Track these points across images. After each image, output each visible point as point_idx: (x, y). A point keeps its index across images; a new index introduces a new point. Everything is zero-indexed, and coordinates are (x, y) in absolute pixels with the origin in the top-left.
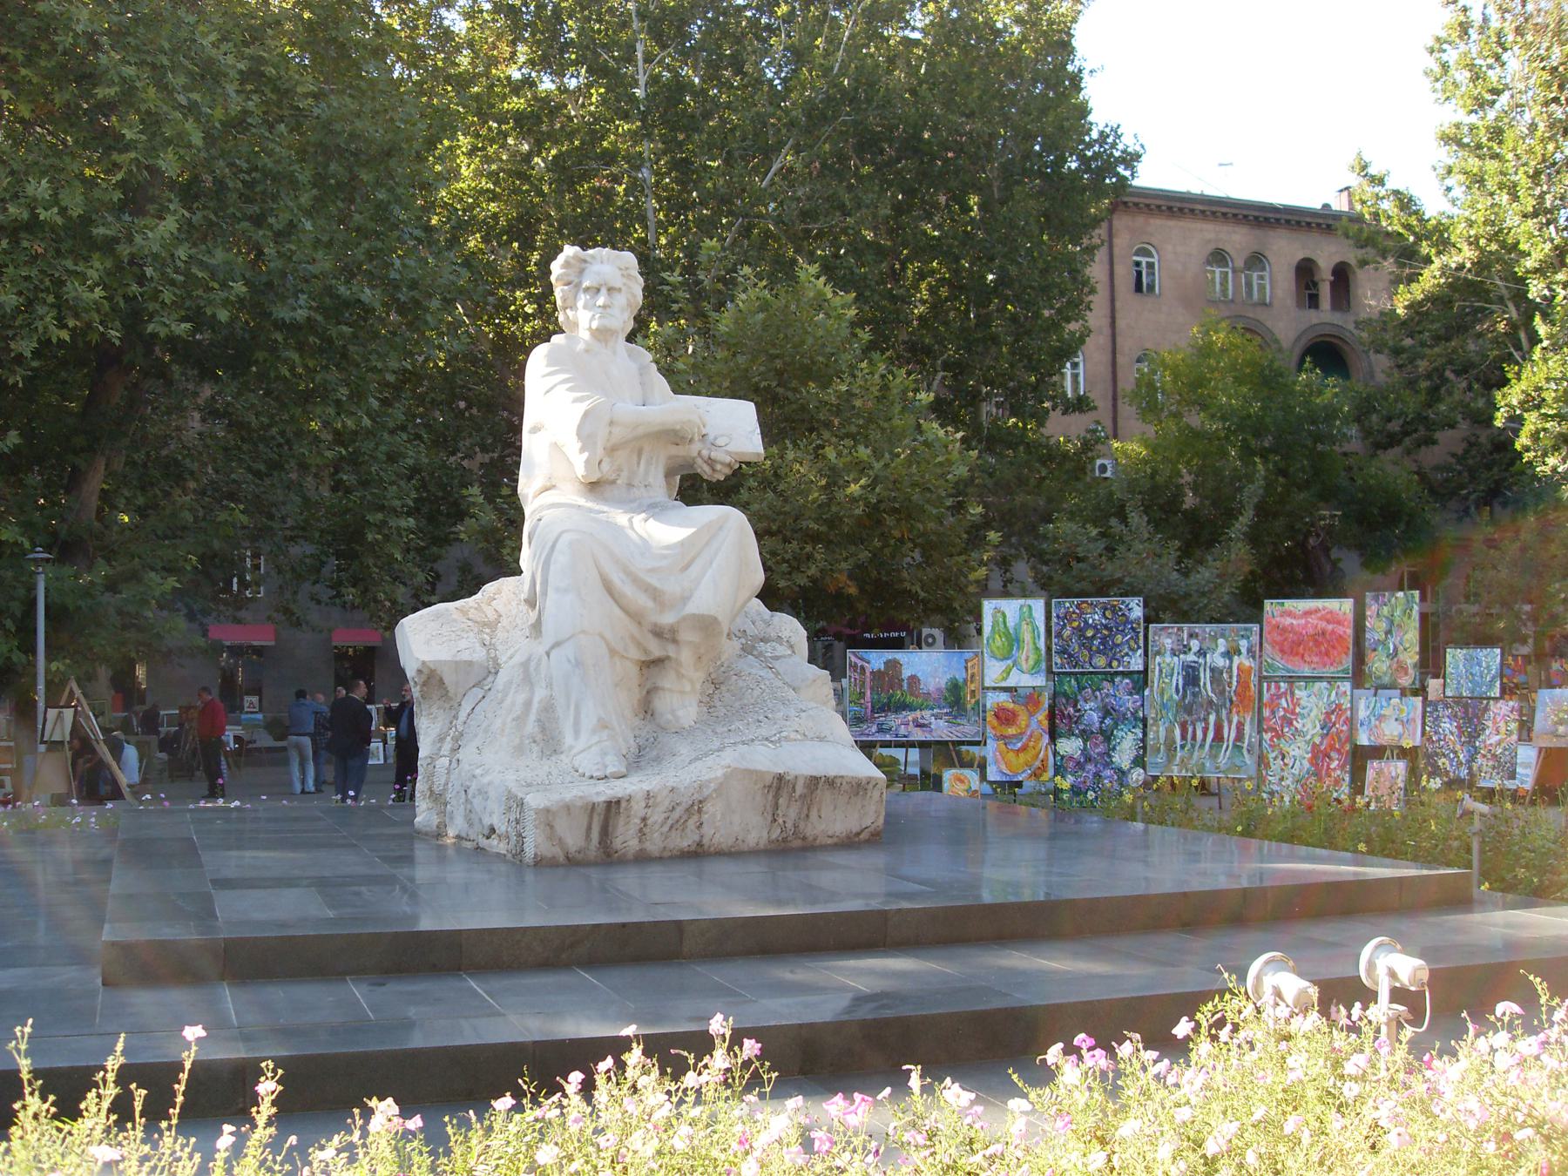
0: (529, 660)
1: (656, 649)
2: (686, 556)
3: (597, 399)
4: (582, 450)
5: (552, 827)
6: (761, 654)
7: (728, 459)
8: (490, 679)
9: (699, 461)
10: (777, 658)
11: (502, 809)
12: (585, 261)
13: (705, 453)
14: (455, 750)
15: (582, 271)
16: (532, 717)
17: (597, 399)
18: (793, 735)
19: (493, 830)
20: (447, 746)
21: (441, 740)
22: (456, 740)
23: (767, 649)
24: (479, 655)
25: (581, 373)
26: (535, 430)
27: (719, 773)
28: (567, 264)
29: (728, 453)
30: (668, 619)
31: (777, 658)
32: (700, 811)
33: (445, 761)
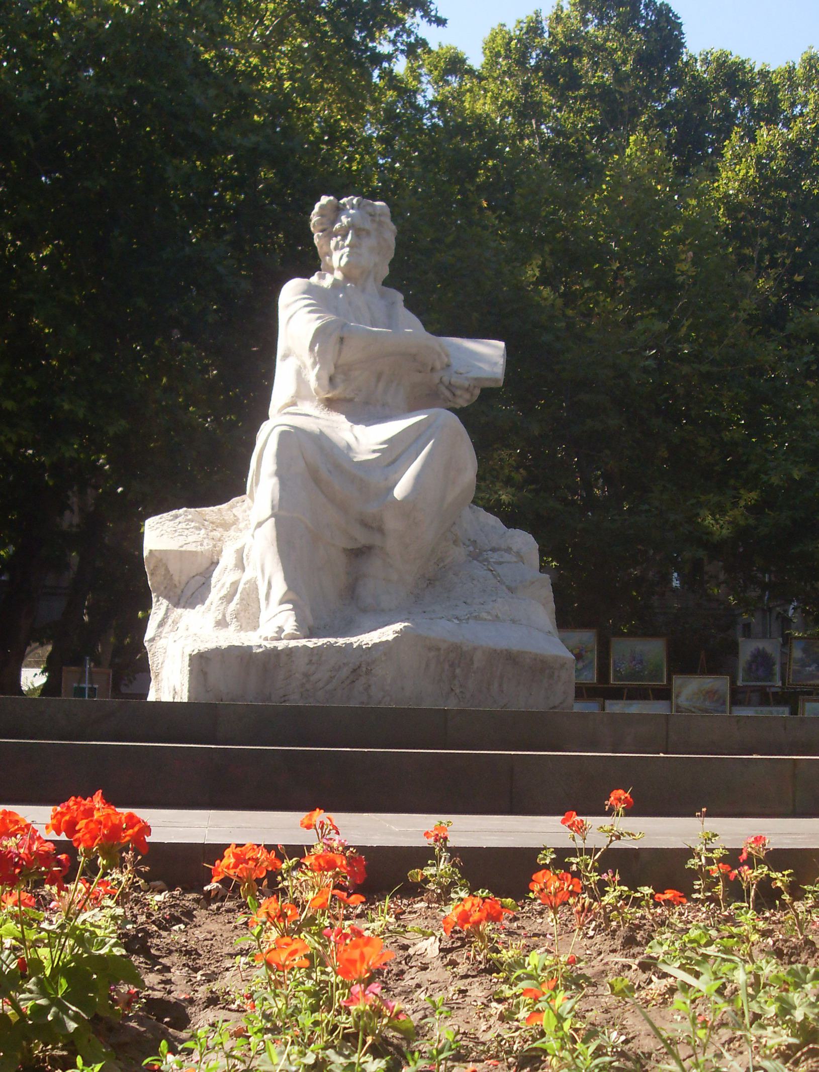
0: (243, 547)
1: (362, 538)
3: (330, 317)
4: (314, 364)
5: (205, 674)
6: (486, 560)
7: (466, 384)
10: (500, 563)
13: (446, 379)
17: (330, 317)
18: (484, 615)
23: (494, 557)
25: (321, 300)
26: (286, 357)
28: (321, 214)
29: (467, 379)
31: (500, 563)
32: (368, 672)
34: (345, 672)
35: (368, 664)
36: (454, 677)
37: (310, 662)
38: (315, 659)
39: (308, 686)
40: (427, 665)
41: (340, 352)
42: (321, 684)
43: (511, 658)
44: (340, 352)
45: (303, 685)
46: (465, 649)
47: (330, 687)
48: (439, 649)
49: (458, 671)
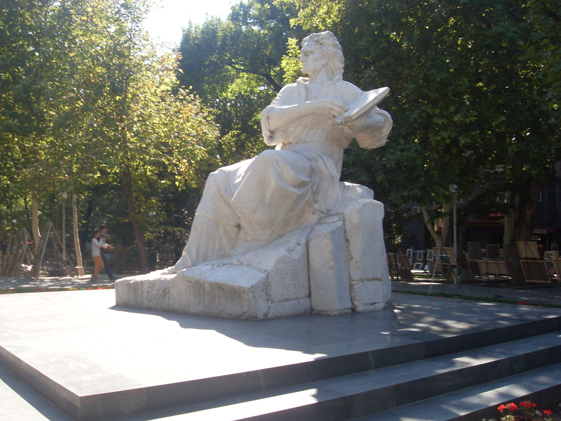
32: (169, 292)
34: (161, 292)
35: (168, 288)
36: (200, 295)
37: (149, 287)
38: (151, 285)
39: (149, 297)
40: (190, 290)
41: (269, 123)
42: (154, 297)
43: (220, 287)
44: (269, 123)
45: (147, 297)
46: (201, 282)
47: (157, 298)
48: (192, 282)
49: (201, 292)
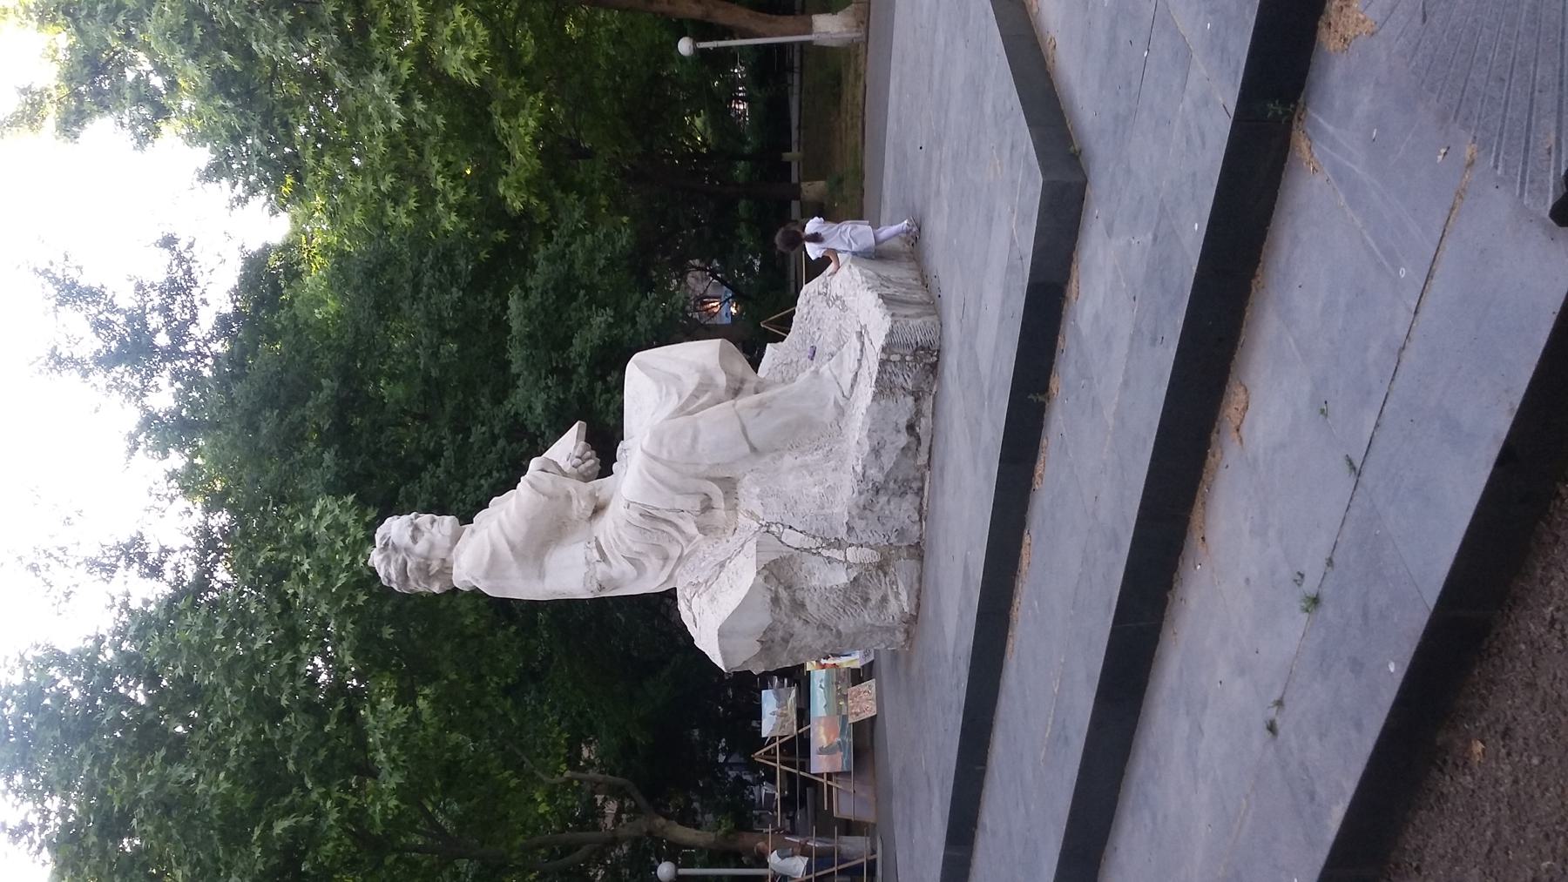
2: (666, 380)
8: (773, 528)
9: (582, 467)
11: (892, 404)
12: (386, 544)
14: (838, 544)
15: (395, 549)
16: (809, 458)
19: (911, 428)
20: (836, 554)
21: (830, 560)
22: (830, 546)
24: (751, 547)
27: (855, 270)
30: (722, 380)
33: (850, 551)
